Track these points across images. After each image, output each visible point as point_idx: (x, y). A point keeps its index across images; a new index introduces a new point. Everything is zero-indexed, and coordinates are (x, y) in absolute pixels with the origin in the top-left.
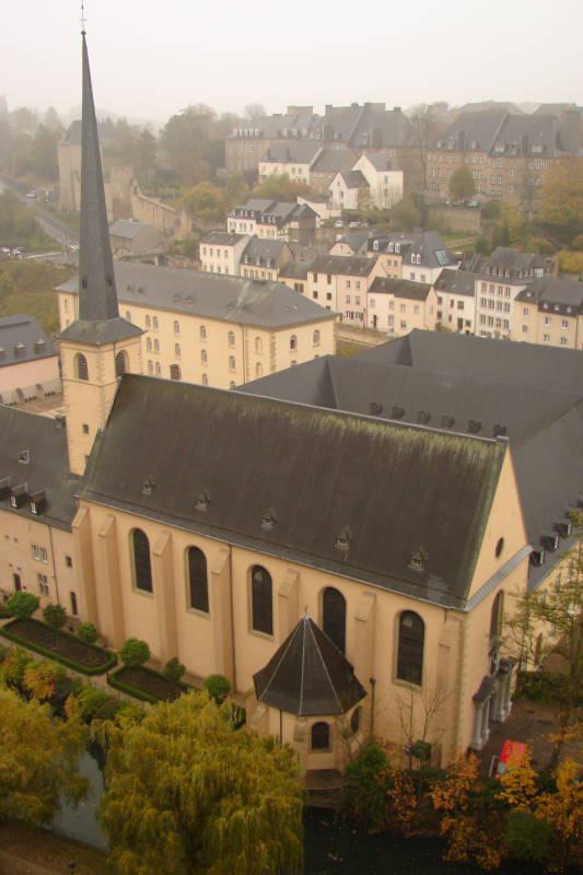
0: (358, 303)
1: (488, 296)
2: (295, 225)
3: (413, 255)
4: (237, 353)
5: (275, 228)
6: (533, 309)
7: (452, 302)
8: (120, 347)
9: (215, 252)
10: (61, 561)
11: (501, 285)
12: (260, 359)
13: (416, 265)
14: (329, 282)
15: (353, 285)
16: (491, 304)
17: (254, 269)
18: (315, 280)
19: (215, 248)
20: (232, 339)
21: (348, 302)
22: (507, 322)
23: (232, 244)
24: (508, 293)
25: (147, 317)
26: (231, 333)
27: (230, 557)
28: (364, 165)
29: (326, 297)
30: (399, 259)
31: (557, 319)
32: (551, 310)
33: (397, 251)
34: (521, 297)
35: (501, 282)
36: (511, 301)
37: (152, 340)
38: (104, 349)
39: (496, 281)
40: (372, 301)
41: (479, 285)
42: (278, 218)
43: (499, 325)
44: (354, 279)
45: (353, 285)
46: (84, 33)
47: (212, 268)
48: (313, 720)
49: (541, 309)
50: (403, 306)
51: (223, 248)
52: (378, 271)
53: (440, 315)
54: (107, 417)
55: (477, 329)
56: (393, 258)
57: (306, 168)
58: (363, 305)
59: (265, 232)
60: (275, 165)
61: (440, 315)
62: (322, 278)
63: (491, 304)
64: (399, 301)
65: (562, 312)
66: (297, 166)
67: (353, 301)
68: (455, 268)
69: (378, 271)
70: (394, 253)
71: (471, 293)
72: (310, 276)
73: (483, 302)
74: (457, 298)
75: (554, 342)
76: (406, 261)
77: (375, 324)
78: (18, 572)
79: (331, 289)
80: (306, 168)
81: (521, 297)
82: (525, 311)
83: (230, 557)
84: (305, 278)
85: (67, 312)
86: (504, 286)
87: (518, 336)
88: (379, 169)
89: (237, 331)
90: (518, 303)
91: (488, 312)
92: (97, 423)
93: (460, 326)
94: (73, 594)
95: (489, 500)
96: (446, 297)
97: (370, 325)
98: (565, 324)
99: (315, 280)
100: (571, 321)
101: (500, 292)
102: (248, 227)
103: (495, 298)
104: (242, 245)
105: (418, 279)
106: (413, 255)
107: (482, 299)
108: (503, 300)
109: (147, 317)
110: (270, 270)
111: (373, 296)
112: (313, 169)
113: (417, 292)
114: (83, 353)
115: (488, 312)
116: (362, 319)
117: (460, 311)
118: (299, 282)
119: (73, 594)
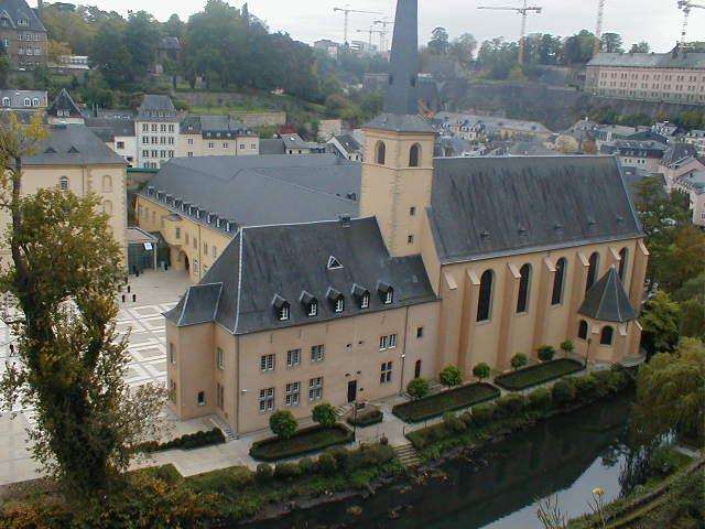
1: (150, 134)
6: (198, 138)
16: (154, 140)
22: (171, 153)
24: (171, 129)
31: (218, 143)
32: (214, 136)
41: (139, 126)
49: (205, 137)
63: (154, 140)
65: (224, 136)
71: (132, 133)
73: (145, 140)
82: (190, 141)
91: (150, 147)
94: (418, 363)
98: (225, 145)
100: (231, 143)
101: (163, 128)
103: (159, 134)
108: (167, 135)
115: (150, 147)
119: (418, 363)
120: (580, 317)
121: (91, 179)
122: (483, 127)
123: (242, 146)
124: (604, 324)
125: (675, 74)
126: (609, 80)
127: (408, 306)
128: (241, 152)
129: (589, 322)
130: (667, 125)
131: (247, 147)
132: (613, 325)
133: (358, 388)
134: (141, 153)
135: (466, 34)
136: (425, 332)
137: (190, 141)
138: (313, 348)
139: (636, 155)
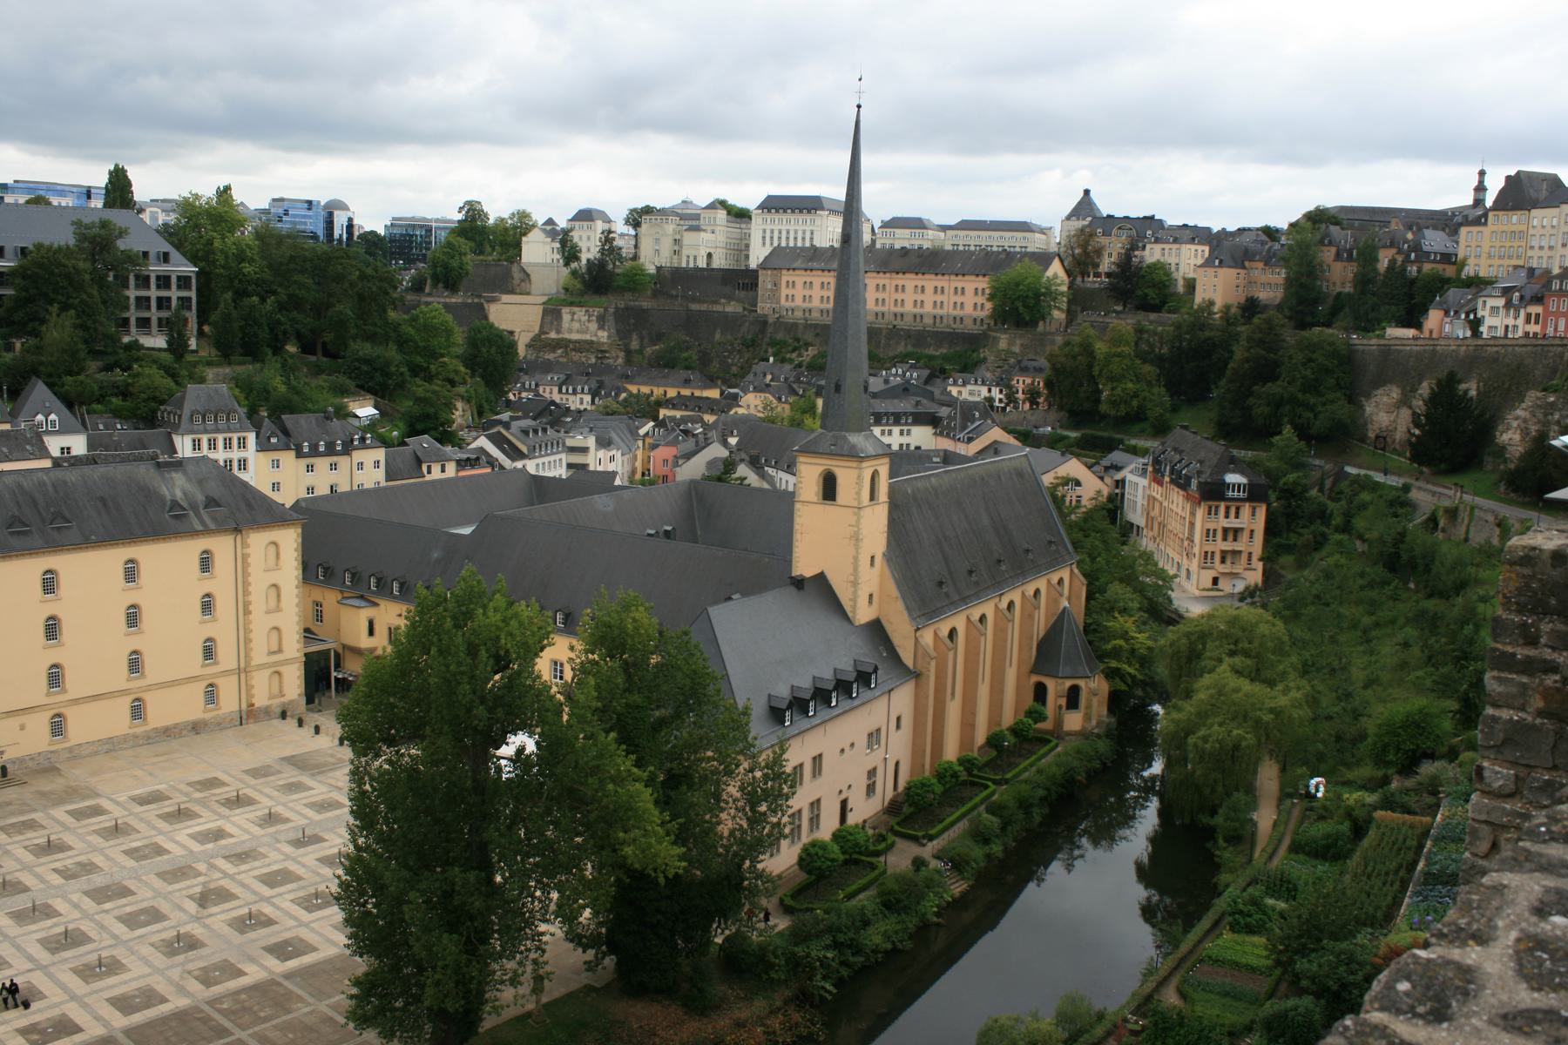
4: (222, 585)
6: (287, 458)
12: (274, 578)
20: (206, 563)
24: (242, 444)
31: (322, 464)
32: (315, 452)
39: (218, 431)
46: (859, 107)
65: (331, 451)
78: (843, 797)
89: (222, 546)
90: (261, 454)
94: (897, 764)
98: (334, 467)
100: (343, 461)
101: (228, 444)
119: (897, 764)
120: (1035, 678)
122: (601, 385)
123: (361, 466)
124: (1068, 683)
125: (910, 281)
126: (799, 292)
127: (890, 691)
129: (1050, 684)
130: (913, 367)
131: (369, 464)
132: (1081, 683)
133: (850, 806)
135: (524, 212)
136: (904, 722)
137: (276, 464)
138: (814, 759)
139: (897, 422)
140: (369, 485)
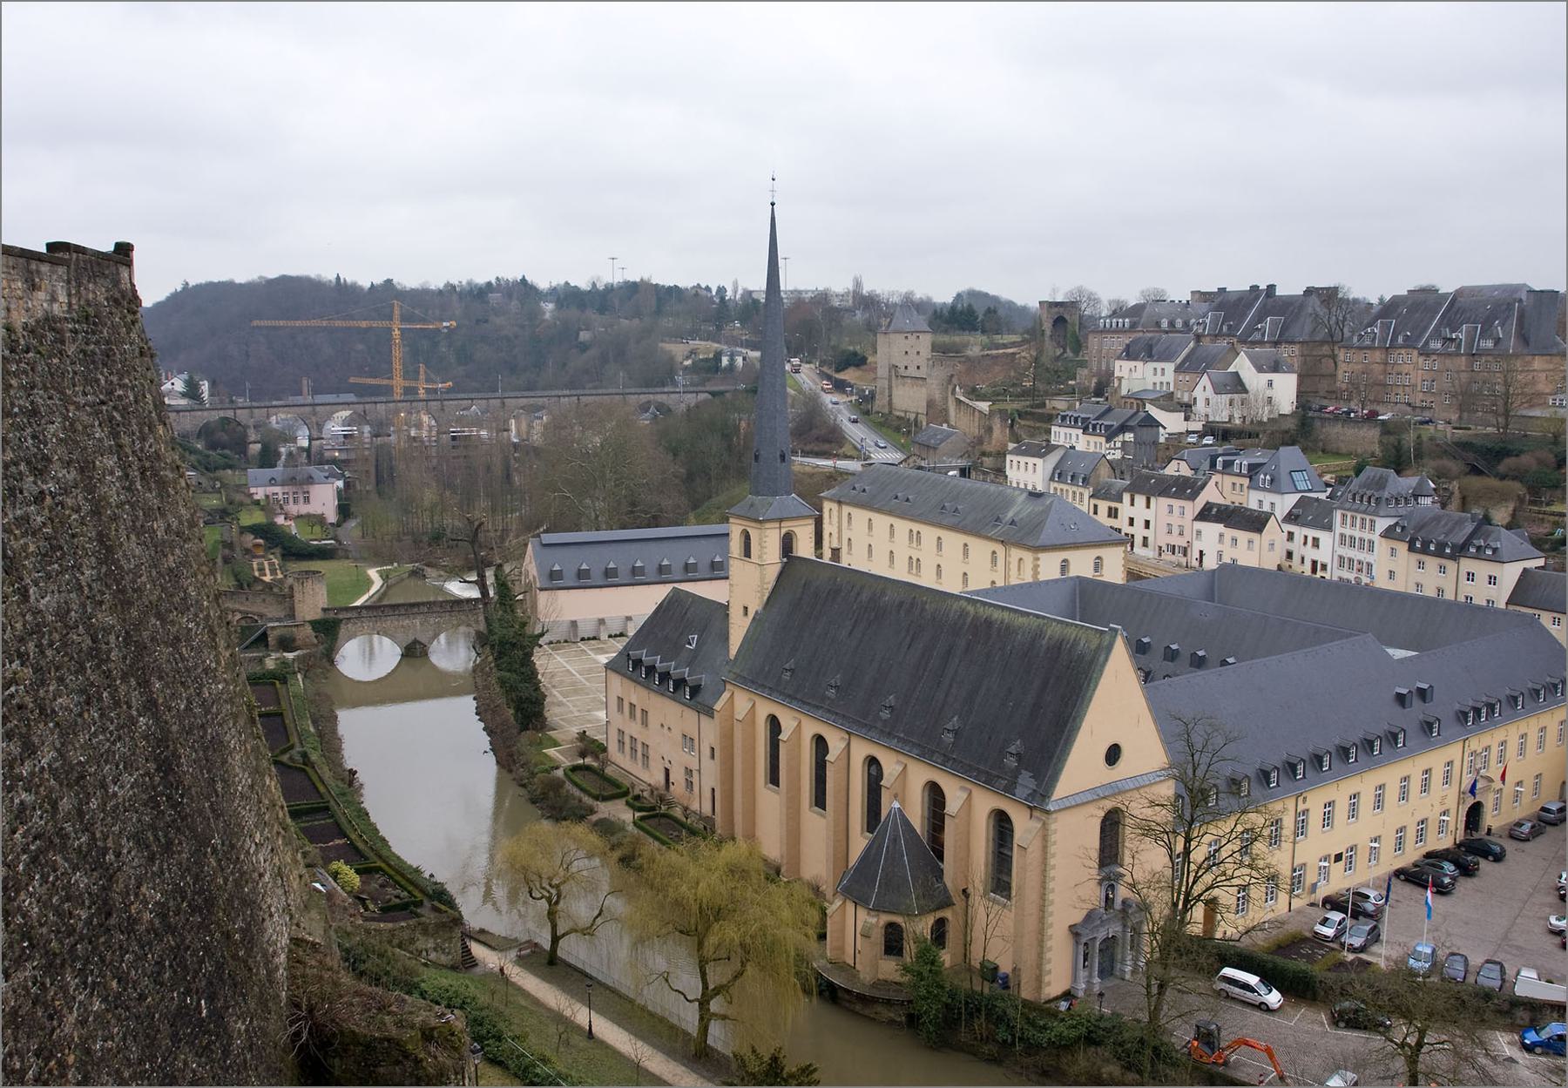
0: (1181, 534)
1: (1348, 532)
2: (1129, 437)
3: (1262, 476)
5: (1103, 440)
6: (1402, 548)
7: (1306, 537)
8: (787, 526)
9: (1022, 465)
10: (706, 752)
11: (1364, 516)
13: (1264, 489)
14: (1148, 506)
15: (1176, 510)
17: (1065, 487)
18: (1132, 504)
19: (1023, 459)
21: (1170, 532)
22: (1369, 565)
23: (1041, 456)
24: (1372, 528)
25: (911, 531)
26: (994, 552)
27: (849, 744)
28: (1242, 365)
29: (1143, 524)
30: (1246, 482)
31: (1432, 563)
32: (1425, 550)
33: (1244, 471)
34: (1388, 534)
35: (1364, 512)
36: (1376, 537)
37: (915, 559)
38: (768, 525)
40: (1199, 533)
42: (1108, 427)
43: (1360, 570)
44: (1176, 503)
45: (1176, 510)
47: (1018, 483)
48: (885, 918)
49: (1411, 549)
50: (1235, 540)
51: (1031, 460)
52: (1210, 494)
53: (1290, 555)
54: (765, 598)
55: (1334, 574)
56: (1239, 480)
57: (1170, 367)
58: (1187, 537)
59: (1084, 443)
60: (1132, 364)
61: (1290, 555)
62: (1140, 500)
64: (1230, 533)
65: (1439, 553)
66: (1159, 365)
67: (1176, 531)
68: (1322, 496)
69: (1210, 494)
70: (1240, 475)
72: (1126, 497)
74: (1312, 533)
75: (1430, 592)
76: (1254, 486)
77: (1201, 561)
78: (668, 766)
79: (1149, 515)
80: (1170, 367)
81: (1388, 534)
82: (1393, 551)
83: (849, 744)
84: (1121, 501)
85: (830, 523)
86: (1368, 518)
87: (1382, 582)
88: (1260, 370)
92: (755, 606)
93: (1314, 570)
95: (1090, 692)
96: (1300, 532)
97: (1195, 564)
98: (1443, 569)
99: (1132, 504)
100: (1451, 565)
101: (1363, 526)
102: (1074, 438)
103: (1357, 534)
104: (1054, 458)
105: (1253, 505)
106: (1262, 476)
107: (1342, 535)
108: (1366, 536)
109: (911, 531)
110: (1081, 490)
111: (1199, 525)
112: (1178, 370)
113: (1255, 522)
114: (749, 530)
116: (1185, 555)
117: (1315, 550)
118: (1114, 505)
121: (1039, 563)
128: (1467, 588)
134: (1336, 558)
140: (1479, 601)
